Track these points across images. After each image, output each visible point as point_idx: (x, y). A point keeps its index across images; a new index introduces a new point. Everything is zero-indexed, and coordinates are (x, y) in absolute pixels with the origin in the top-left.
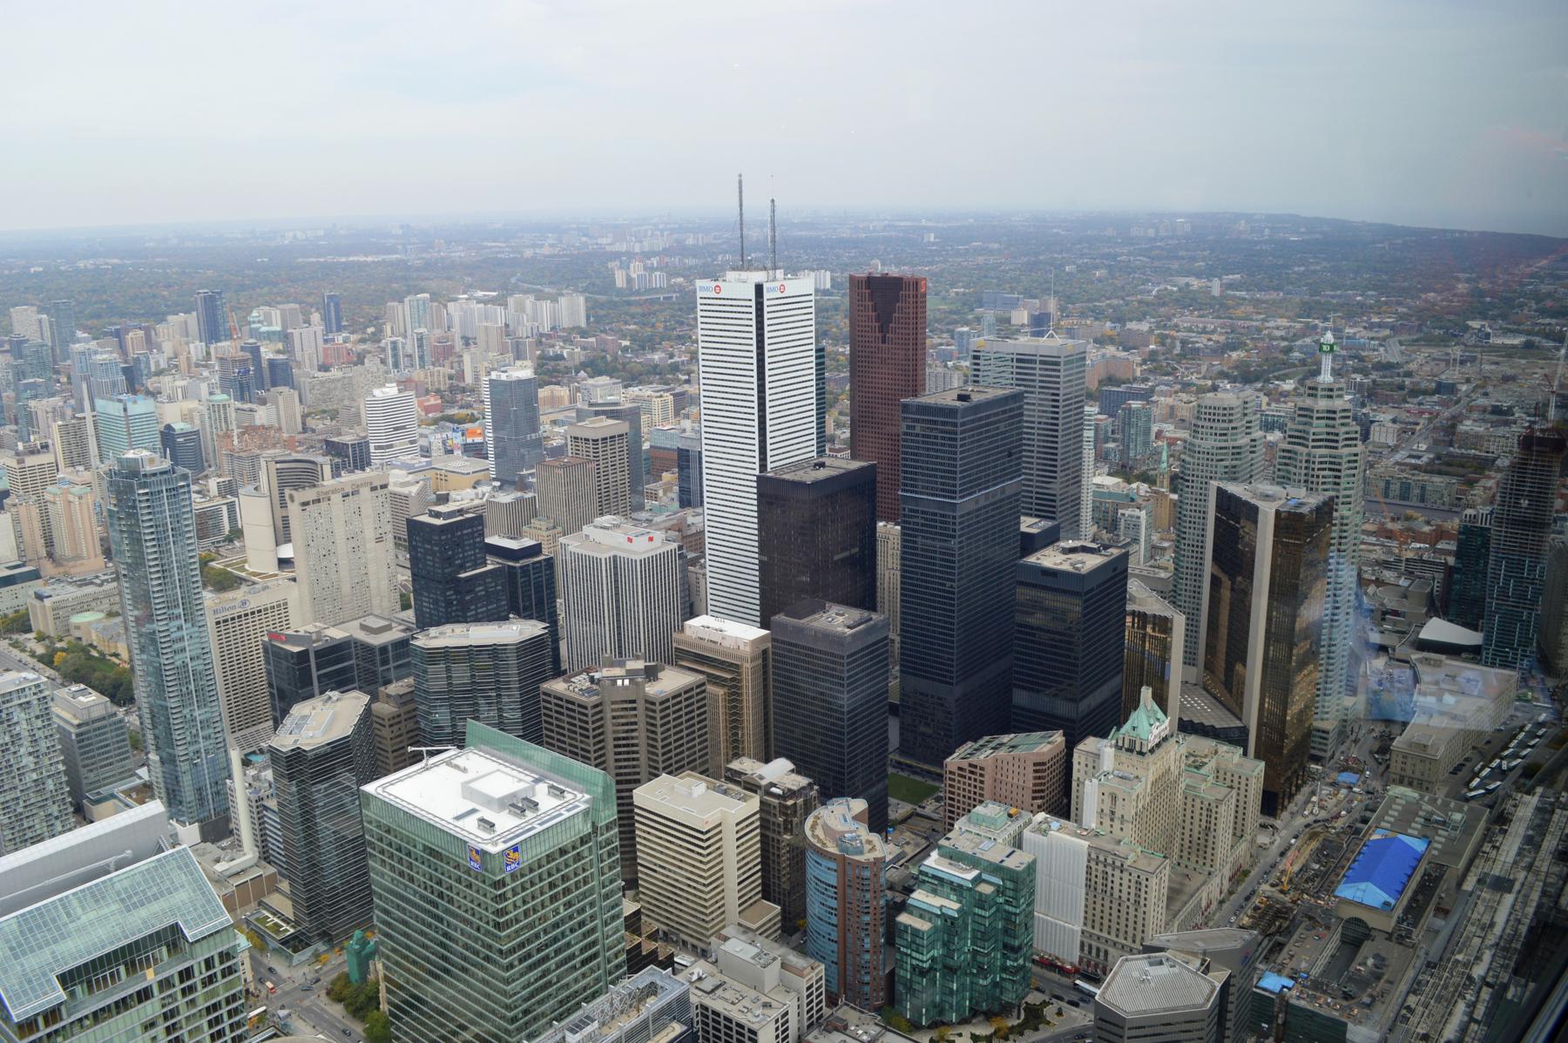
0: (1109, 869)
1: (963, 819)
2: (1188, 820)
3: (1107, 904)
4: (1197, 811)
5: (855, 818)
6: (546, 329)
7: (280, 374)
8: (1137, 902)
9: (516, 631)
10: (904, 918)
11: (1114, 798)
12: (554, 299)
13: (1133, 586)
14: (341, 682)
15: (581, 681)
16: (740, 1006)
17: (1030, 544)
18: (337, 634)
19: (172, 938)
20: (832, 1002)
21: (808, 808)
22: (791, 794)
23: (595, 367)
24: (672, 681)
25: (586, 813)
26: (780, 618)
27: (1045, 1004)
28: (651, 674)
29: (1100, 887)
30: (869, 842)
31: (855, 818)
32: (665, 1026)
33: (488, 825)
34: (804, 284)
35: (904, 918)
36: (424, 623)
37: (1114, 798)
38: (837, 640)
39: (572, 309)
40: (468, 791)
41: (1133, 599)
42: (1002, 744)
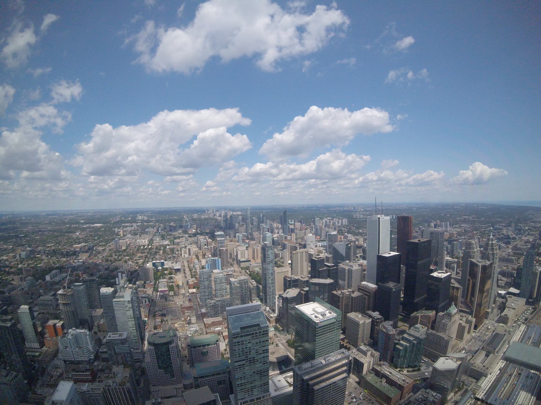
6: (340, 225)
7: (292, 231)
9: (329, 281)
10: (397, 346)
12: (342, 219)
13: (452, 281)
14: (296, 286)
15: (339, 292)
17: (432, 271)
18: (296, 278)
19: (258, 325)
20: (380, 361)
21: (381, 322)
22: (378, 319)
23: (348, 233)
24: (356, 294)
25: (335, 318)
26: (380, 283)
28: (353, 292)
33: (316, 317)
34: (388, 218)
35: (397, 346)
36: (312, 277)
38: (391, 289)
39: (345, 221)
40: (314, 310)
41: (452, 283)
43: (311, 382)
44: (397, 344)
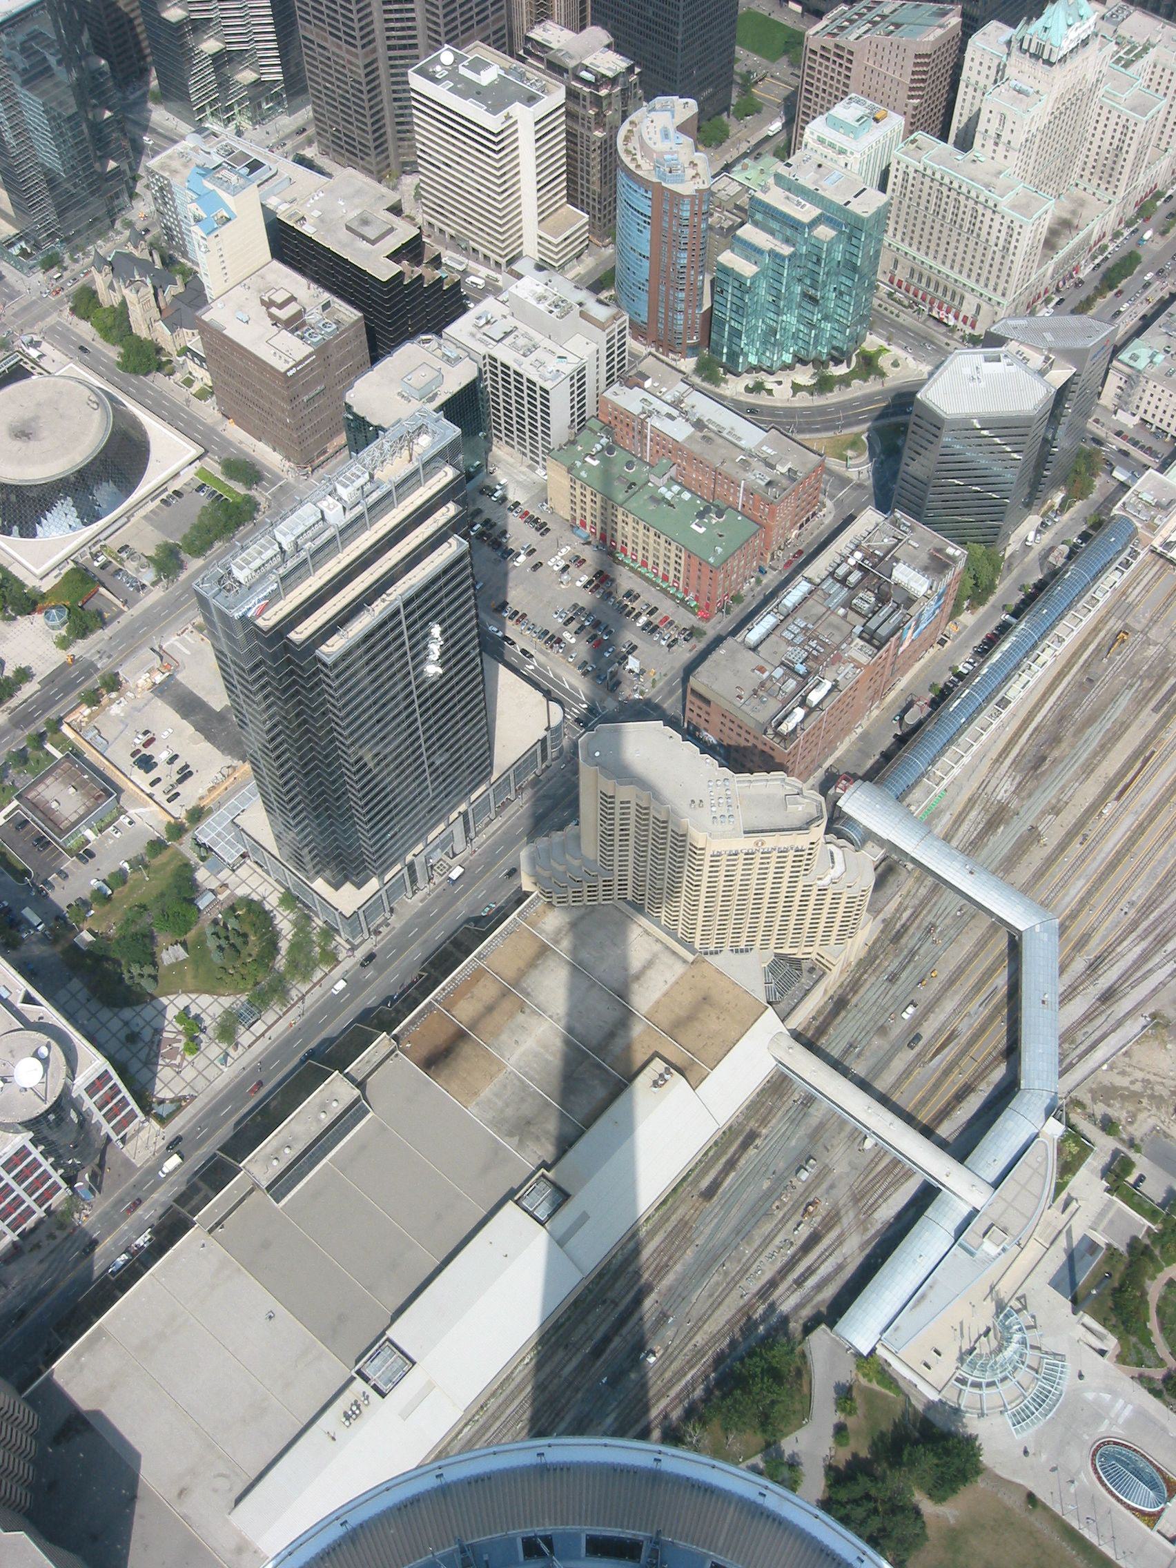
0: (980, 208)
1: (820, 120)
2: (1098, 137)
3: (971, 245)
4: (1111, 126)
5: (681, 128)
8: (1005, 249)
11: (1003, 119)
16: (532, 357)
27: (881, 351)
29: (966, 225)
30: (693, 164)
31: (681, 128)
32: (437, 469)
35: (728, 258)
37: (1003, 119)
42: (883, 17)
43: (299, 634)
44: (729, 235)
